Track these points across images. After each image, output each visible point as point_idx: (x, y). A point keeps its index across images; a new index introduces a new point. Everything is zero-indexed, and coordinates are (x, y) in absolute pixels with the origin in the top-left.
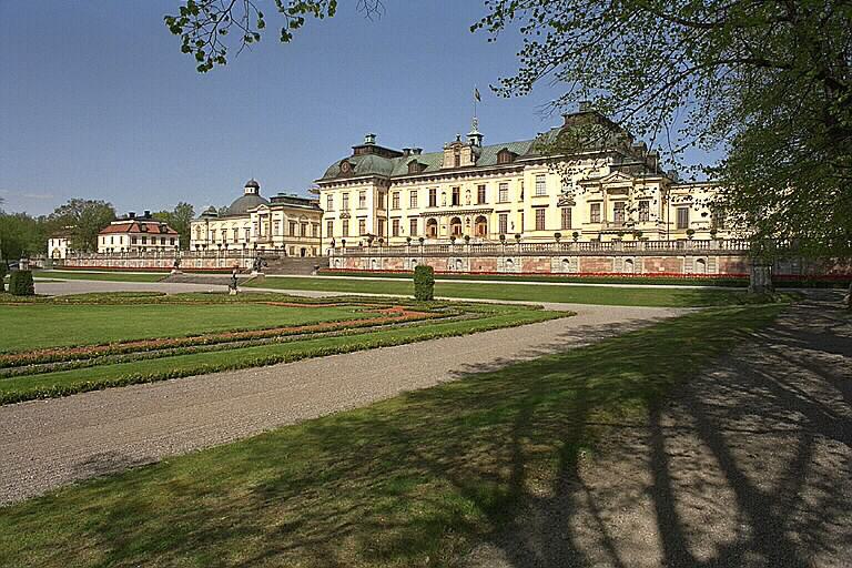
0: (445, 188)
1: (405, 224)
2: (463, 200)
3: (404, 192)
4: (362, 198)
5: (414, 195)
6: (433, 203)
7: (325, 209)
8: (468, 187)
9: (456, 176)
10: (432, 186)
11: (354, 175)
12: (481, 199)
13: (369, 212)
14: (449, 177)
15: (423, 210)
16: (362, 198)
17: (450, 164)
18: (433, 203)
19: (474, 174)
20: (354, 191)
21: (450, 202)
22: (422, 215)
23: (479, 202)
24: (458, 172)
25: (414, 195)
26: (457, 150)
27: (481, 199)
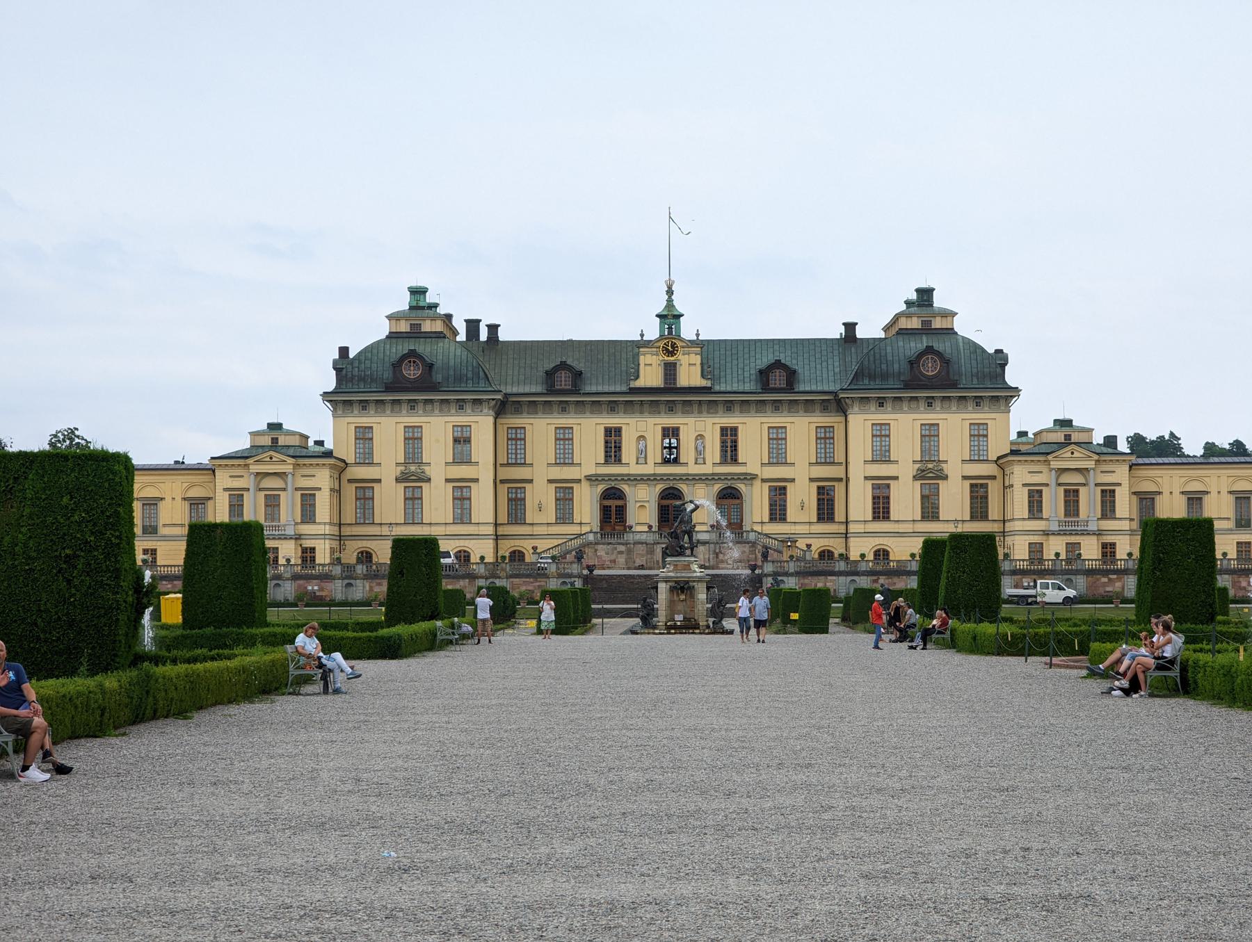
0: (643, 431)
1: (541, 497)
2: (687, 454)
3: (540, 430)
4: (462, 440)
5: (564, 438)
6: (613, 450)
7: (350, 460)
8: (698, 431)
9: (671, 408)
10: (613, 421)
11: (434, 388)
12: (730, 449)
14: (654, 408)
15: (592, 470)
16: (462, 440)
17: (650, 374)
18: (613, 450)
19: (712, 407)
20: (437, 429)
21: (655, 454)
22: (589, 478)
23: (724, 461)
24: (670, 396)
25: (564, 438)
26: (671, 353)
27: (730, 449)
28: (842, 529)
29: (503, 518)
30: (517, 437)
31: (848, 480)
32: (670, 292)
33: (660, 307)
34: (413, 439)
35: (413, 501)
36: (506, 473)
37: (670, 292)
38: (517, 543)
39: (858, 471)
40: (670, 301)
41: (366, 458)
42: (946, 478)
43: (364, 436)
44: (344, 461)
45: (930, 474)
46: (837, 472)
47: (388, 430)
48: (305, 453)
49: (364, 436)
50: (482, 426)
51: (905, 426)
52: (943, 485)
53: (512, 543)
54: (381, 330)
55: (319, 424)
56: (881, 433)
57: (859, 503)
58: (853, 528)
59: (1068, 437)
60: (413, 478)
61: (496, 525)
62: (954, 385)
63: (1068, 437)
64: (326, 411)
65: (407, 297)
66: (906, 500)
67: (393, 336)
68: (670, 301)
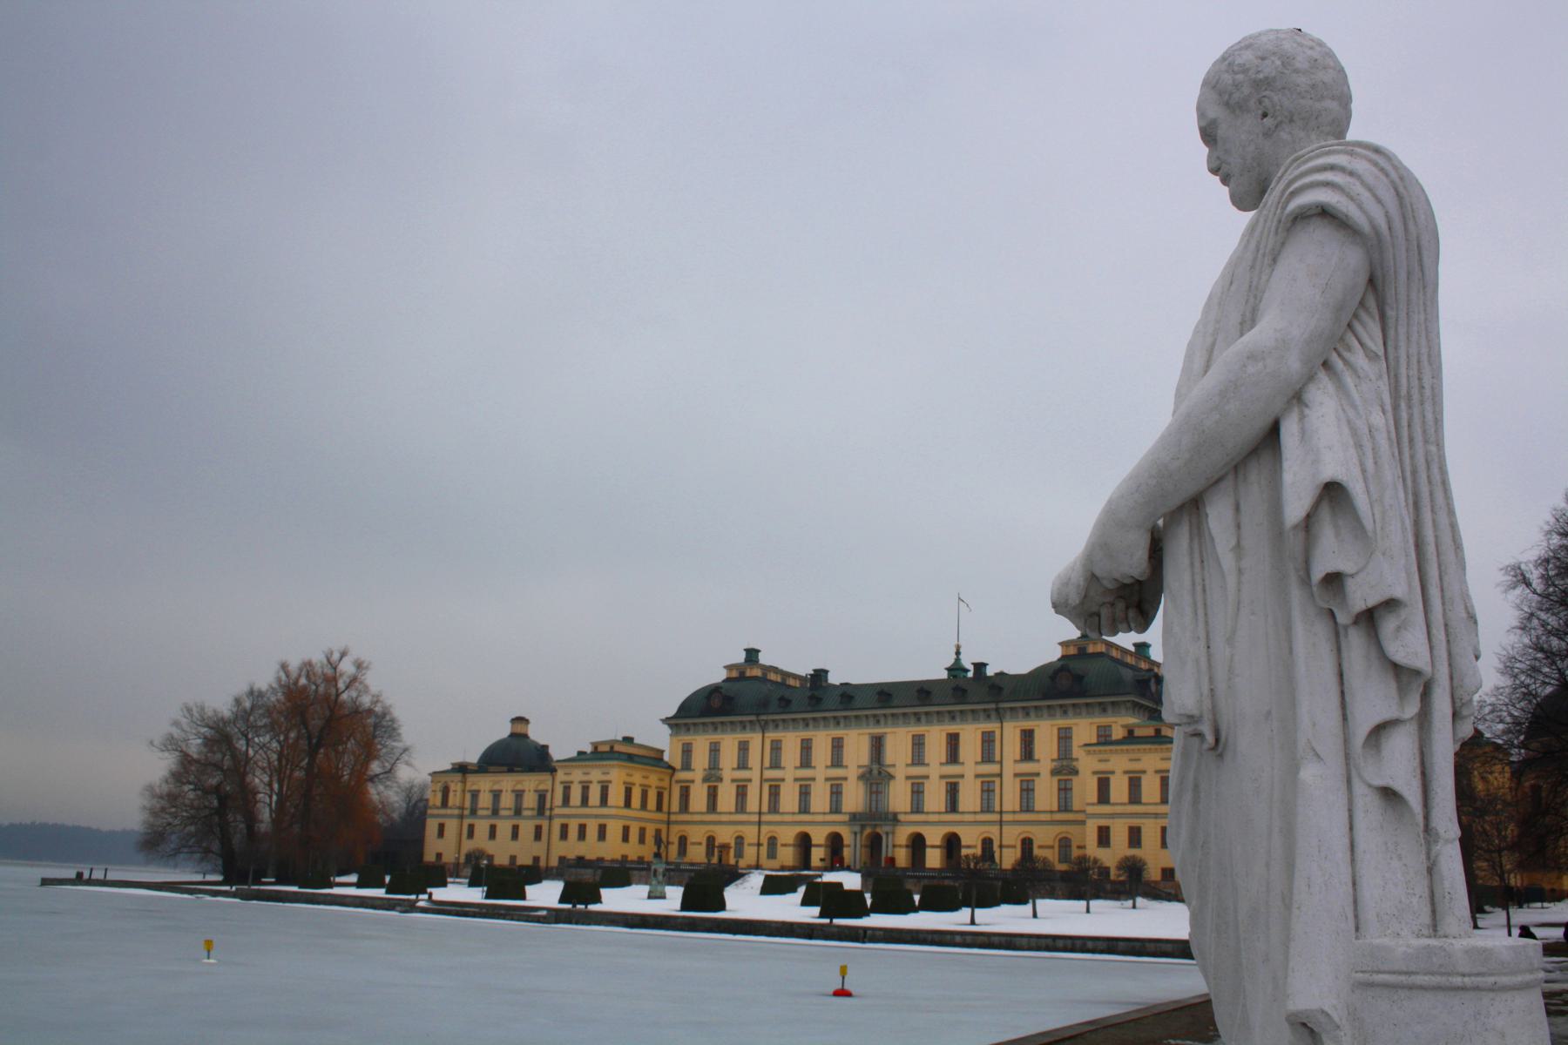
7: (677, 764)
13: (754, 774)
20: (729, 743)
28: (996, 817)
29: (765, 808)
30: (776, 747)
31: (1000, 775)
32: (958, 653)
33: (950, 661)
34: (715, 750)
35: (713, 795)
36: (769, 774)
37: (958, 653)
38: (740, 828)
39: (1010, 768)
40: (958, 660)
41: (687, 766)
42: (1076, 772)
43: (687, 751)
44: (670, 767)
45: (1065, 769)
46: (994, 768)
47: (701, 744)
48: (654, 759)
49: (687, 751)
50: (755, 739)
51: (1046, 732)
52: (1074, 778)
53: (772, 828)
54: (719, 676)
55: (659, 738)
56: (1028, 737)
57: (1010, 796)
58: (1006, 817)
59: (1158, 731)
60: (713, 776)
61: (760, 813)
62: (1083, 694)
63: (1158, 731)
64: (666, 730)
65: (743, 655)
66: (1046, 794)
67: (728, 680)
68: (958, 660)
